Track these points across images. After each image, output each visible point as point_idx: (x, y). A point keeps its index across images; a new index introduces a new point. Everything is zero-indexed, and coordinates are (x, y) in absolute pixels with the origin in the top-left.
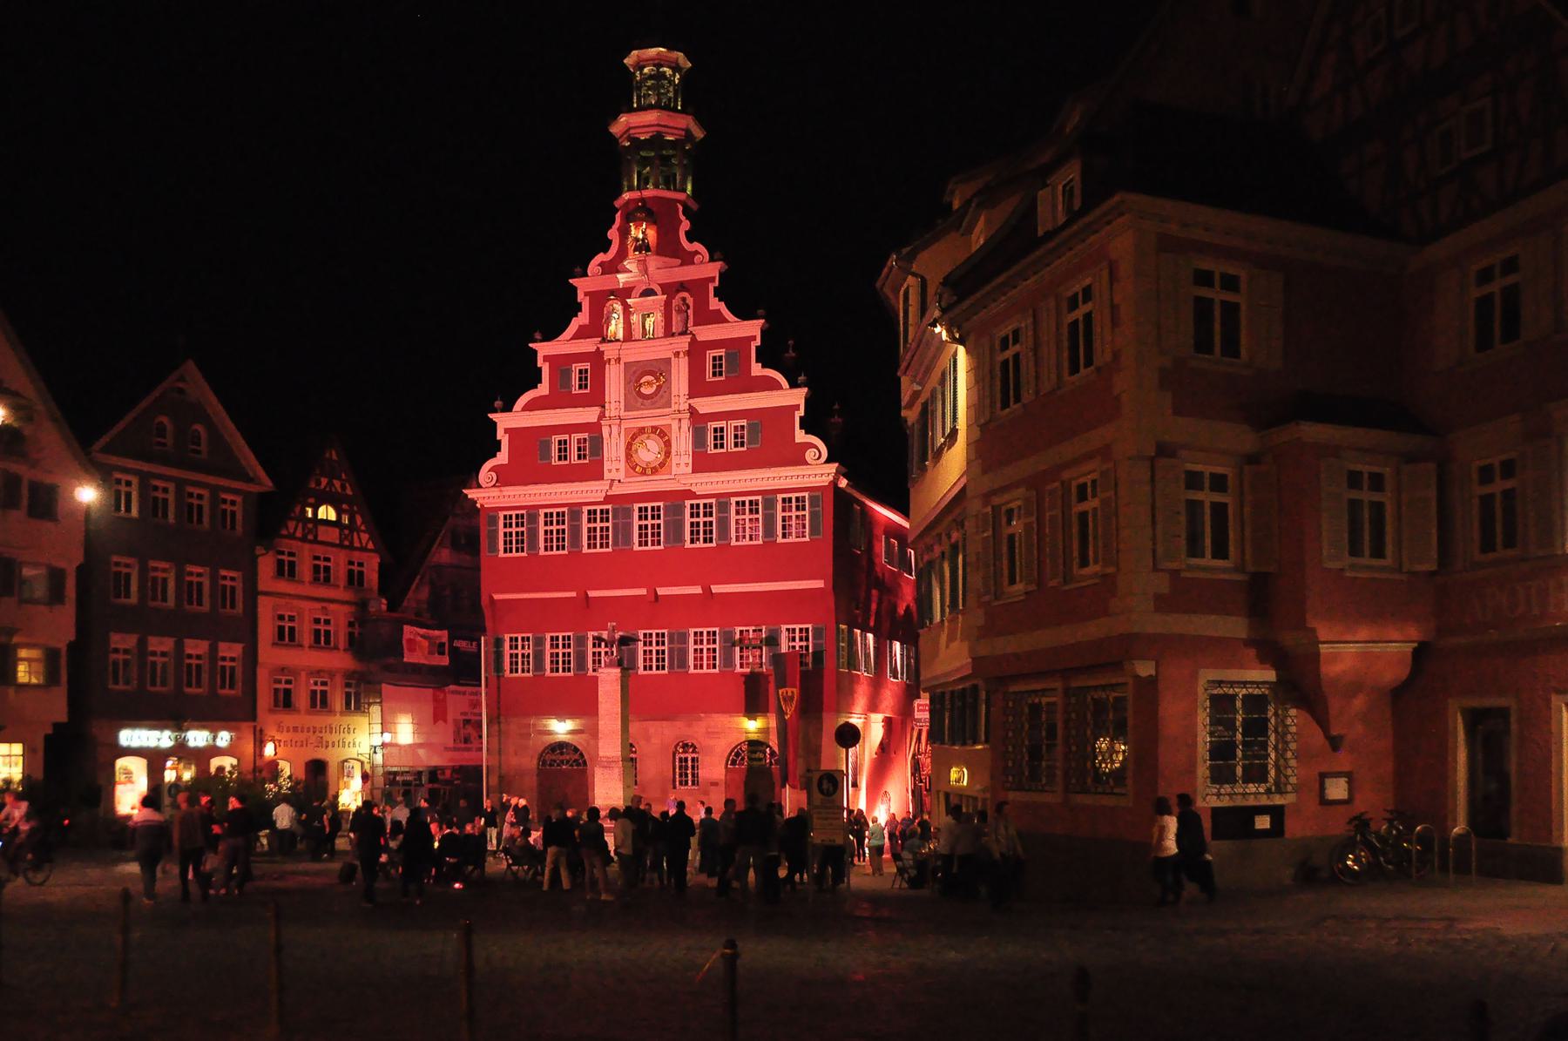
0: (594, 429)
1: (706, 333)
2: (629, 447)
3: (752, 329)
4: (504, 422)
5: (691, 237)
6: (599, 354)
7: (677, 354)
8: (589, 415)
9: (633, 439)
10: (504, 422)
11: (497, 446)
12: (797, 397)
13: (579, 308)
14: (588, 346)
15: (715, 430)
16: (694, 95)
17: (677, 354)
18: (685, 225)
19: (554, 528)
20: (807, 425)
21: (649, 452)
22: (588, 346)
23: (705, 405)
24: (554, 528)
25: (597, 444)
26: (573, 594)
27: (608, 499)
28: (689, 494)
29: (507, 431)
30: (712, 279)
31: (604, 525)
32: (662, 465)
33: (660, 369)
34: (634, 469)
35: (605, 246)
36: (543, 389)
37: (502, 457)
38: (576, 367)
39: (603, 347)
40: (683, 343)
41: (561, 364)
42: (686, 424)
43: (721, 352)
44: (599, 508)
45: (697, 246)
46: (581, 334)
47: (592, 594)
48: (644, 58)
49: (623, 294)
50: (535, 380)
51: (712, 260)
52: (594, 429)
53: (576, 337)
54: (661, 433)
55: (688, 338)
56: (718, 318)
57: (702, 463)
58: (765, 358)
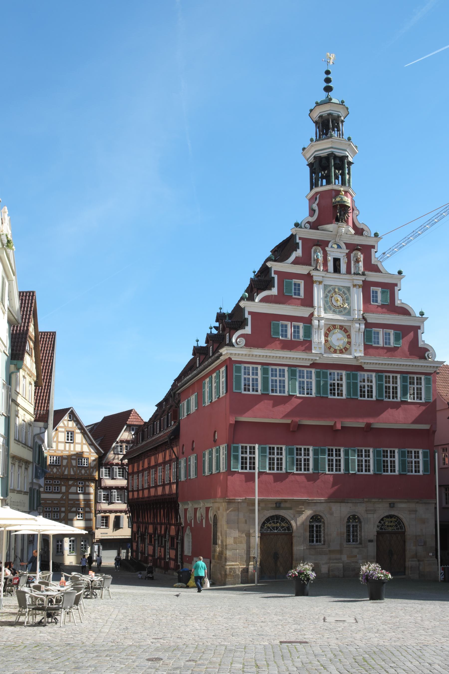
0: (308, 321)
2: (326, 335)
7: (355, 286)
8: (304, 312)
9: (329, 330)
14: (303, 270)
21: (338, 339)
22: (303, 270)
25: (308, 332)
28: (360, 368)
29: (250, 313)
31: (274, 378)
32: (346, 349)
33: (345, 292)
34: (330, 348)
36: (274, 291)
37: (248, 330)
39: (313, 273)
40: (359, 280)
42: (363, 327)
44: (305, 370)
49: (322, 244)
53: (295, 262)
54: (345, 330)
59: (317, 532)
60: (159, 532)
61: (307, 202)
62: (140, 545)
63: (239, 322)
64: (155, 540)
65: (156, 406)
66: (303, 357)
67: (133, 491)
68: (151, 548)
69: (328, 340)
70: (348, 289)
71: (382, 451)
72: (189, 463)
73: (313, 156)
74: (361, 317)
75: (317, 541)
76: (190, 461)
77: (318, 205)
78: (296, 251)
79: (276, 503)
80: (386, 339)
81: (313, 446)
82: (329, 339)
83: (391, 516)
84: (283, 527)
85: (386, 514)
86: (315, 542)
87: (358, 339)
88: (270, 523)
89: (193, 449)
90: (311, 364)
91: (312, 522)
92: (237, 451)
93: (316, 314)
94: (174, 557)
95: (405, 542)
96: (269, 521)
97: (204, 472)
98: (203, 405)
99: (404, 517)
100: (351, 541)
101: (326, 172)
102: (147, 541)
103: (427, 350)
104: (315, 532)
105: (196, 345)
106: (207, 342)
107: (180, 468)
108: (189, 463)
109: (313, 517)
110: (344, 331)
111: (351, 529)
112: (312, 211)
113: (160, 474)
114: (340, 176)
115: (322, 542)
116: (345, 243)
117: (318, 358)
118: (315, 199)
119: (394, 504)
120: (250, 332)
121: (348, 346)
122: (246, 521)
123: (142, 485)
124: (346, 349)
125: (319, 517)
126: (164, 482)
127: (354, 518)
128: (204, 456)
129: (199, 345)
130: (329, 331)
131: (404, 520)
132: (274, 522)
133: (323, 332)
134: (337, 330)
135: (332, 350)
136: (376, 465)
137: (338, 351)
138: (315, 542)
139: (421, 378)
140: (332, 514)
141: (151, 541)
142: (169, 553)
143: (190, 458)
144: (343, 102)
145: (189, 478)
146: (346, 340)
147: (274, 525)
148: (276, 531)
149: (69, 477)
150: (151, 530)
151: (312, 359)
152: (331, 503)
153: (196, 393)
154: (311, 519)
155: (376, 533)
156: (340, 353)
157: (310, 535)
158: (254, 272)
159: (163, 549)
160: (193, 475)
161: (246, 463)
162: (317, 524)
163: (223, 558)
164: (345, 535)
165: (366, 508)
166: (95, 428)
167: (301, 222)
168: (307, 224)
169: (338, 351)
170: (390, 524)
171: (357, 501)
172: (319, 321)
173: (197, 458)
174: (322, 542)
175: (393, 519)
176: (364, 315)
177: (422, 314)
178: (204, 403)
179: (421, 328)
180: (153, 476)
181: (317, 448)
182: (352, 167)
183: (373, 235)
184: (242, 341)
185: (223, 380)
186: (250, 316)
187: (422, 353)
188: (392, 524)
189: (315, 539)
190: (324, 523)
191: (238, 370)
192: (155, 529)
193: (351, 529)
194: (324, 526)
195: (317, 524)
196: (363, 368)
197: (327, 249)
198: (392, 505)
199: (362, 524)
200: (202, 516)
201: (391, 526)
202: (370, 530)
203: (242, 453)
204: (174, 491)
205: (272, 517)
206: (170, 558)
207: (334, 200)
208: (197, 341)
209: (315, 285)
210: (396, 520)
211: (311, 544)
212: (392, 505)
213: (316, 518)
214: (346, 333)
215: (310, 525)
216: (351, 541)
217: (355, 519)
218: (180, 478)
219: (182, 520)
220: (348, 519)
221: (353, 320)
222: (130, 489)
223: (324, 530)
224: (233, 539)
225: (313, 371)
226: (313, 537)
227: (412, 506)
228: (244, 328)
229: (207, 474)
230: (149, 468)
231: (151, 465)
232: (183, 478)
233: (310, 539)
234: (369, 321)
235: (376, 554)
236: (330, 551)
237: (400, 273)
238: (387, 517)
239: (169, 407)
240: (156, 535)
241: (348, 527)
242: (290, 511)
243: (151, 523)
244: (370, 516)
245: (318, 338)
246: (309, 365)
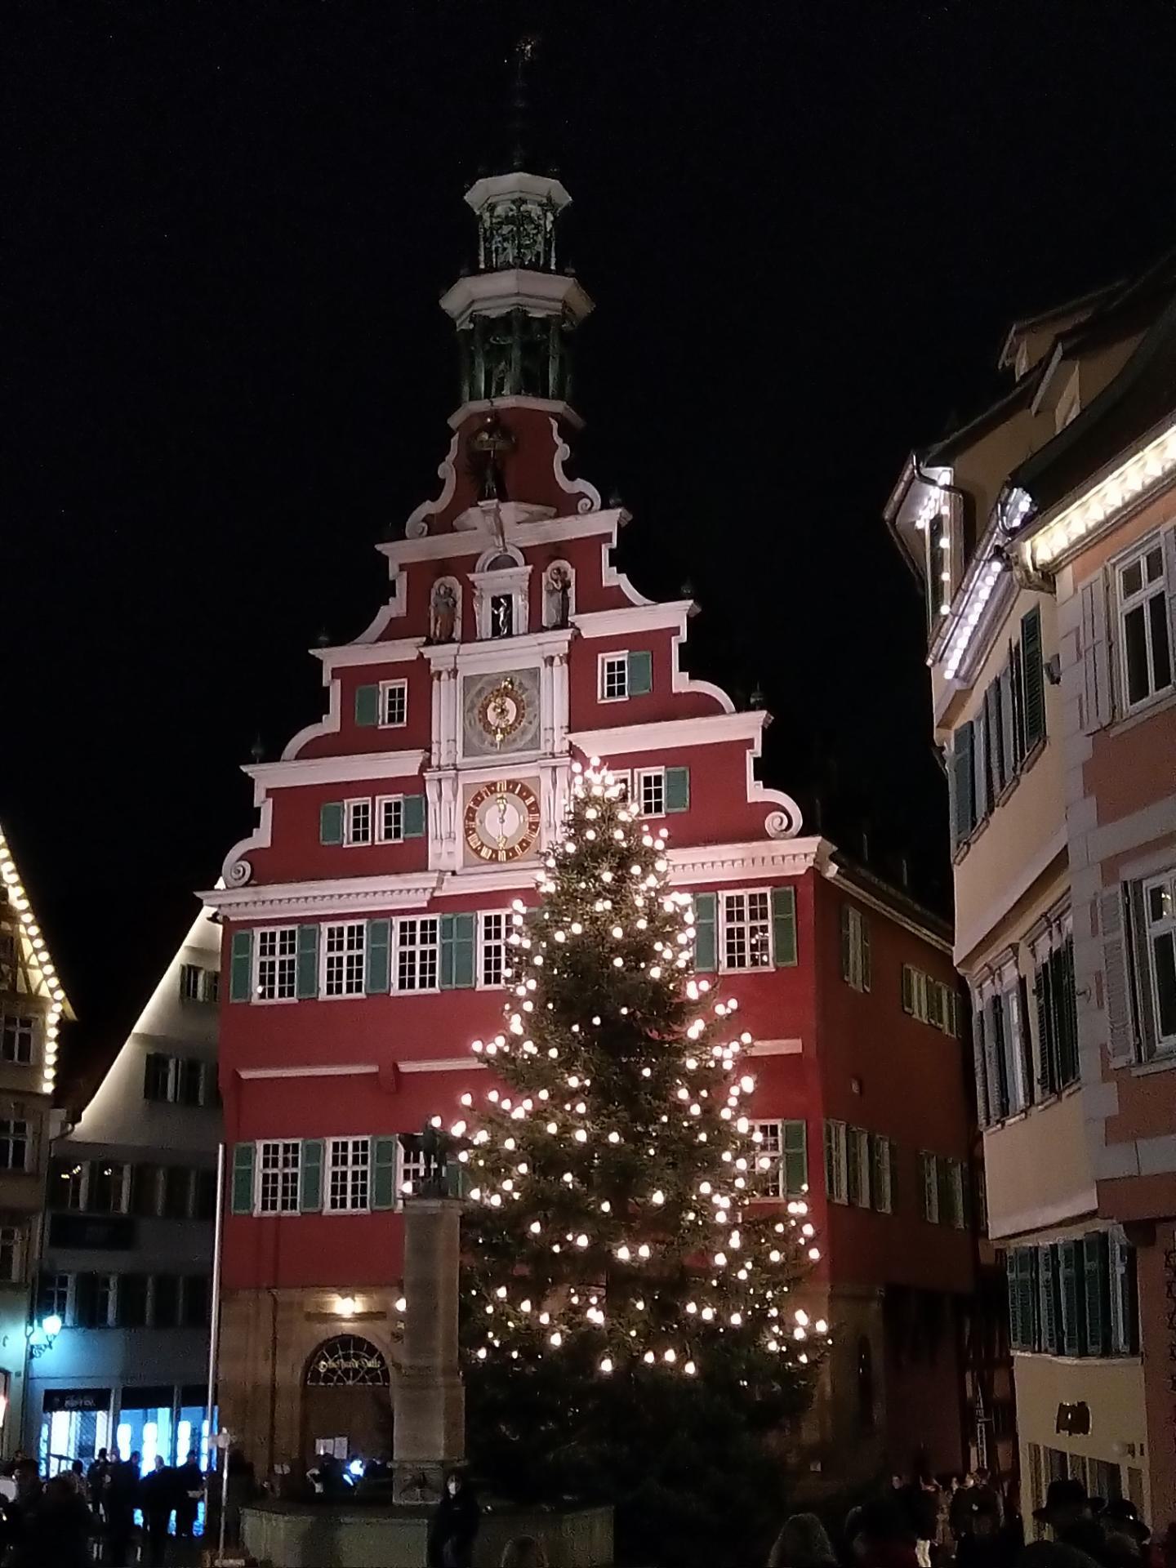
0: (414, 785)
1: (596, 625)
2: (470, 815)
3: (674, 615)
4: (266, 777)
5: (571, 472)
6: (423, 662)
7: (550, 661)
8: (404, 763)
10: (266, 777)
11: (252, 819)
12: (746, 727)
13: (390, 590)
14: (405, 651)
15: (611, 666)
16: (573, 244)
17: (550, 661)
18: (563, 452)
19: (345, 954)
20: (768, 773)
22: (405, 651)
24: (345, 954)
25: (419, 813)
26: (373, 1069)
27: (435, 904)
30: (607, 537)
31: (428, 947)
32: (524, 844)
34: (477, 852)
35: (434, 489)
36: (331, 723)
37: (262, 837)
38: (386, 686)
39: (429, 652)
41: (358, 679)
43: (622, 656)
44: (419, 919)
45: (582, 485)
46: (394, 632)
47: (406, 1067)
48: (495, 192)
50: (319, 709)
51: (605, 506)
52: (414, 785)
54: (523, 791)
55: (567, 634)
56: (616, 600)
58: (694, 664)
66: (246, 899)
69: (474, 830)
70: (534, 673)
93: (434, 762)
110: (519, 794)
116: (521, 549)
120: (267, 843)
130: (477, 802)
147: (344, 1365)
148: (350, 1382)
169: (502, 856)
197: (472, 577)
209: (435, 682)
214: (524, 799)
225: (435, 917)
242: (379, 1323)
246: (425, 905)
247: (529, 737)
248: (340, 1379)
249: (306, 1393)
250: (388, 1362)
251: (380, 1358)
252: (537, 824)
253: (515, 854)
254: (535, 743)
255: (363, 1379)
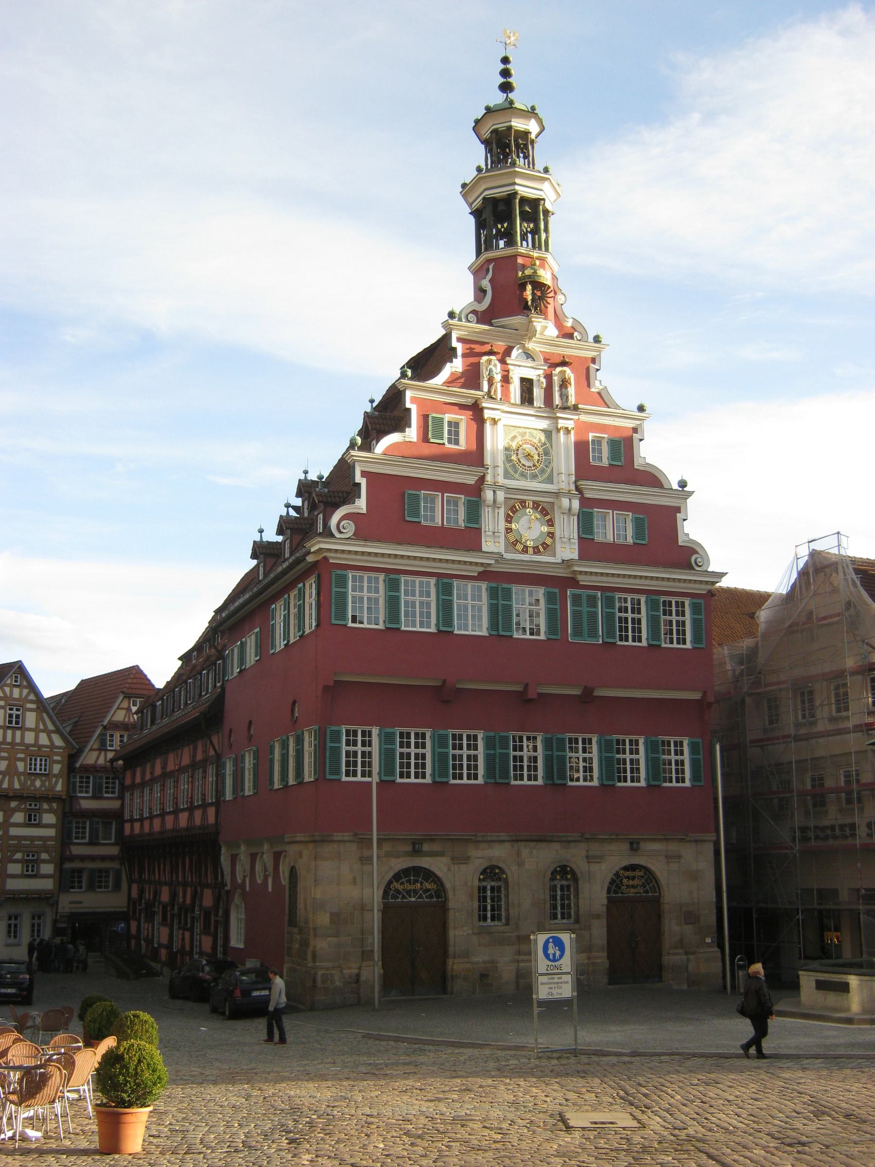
0: (475, 491)
2: (509, 519)
21: (530, 527)
23: (595, 490)
25: (474, 512)
28: (572, 582)
29: (364, 474)
34: (514, 543)
36: (412, 433)
37: (361, 504)
42: (576, 504)
54: (545, 511)
57: (589, 548)
59: (492, 899)
60: (181, 900)
61: (471, 278)
62: (144, 926)
63: (342, 492)
64: (173, 916)
65: (180, 659)
67: (132, 821)
68: (165, 931)
71: (615, 742)
72: (242, 765)
73: (481, 198)
74: (573, 487)
75: (493, 918)
76: (243, 761)
77: (490, 281)
78: (451, 362)
79: (414, 844)
80: (619, 530)
81: (485, 730)
82: (513, 526)
83: (633, 867)
84: (427, 890)
85: (625, 863)
86: (489, 920)
87: (567, 530)
88: (402, 883)
89: (250, 738)
90: (480, 573)
91: (483, 880)
92: (339, 740)
93: (489, 478)
94: (209, 950)
95: (659, 916)
96: (401, 878)
97: (272, 782)
98: (272, 652)
99: (658, 867)
100: (559, 916)
101: (505, 225)
102: (158, 918)
103: (695, 552)
104: (489, 901)
105: (258, 539)
106: (280, 532)
107: (224, 774)
108: (242, 765)
109: (485, 870)
110: (541, 511)
111: (559, 893)
112: (480, 292)
113: (184, 786)
114: (530, 236)
115: (504, 920)
117: (493, 562)
118: (485, 271)
119: (638, 843)
121: (549, 541)
122: (354, 879)
123: (150, 809)
124: (545, 546)
125: (497, 871)
126: (192, 803)
127: (563, 871)
128: (272, 751)
129: (264, 540)
130: (514, 513)
131: (658, 874)
132: (409, 881)
133: (502, 512)
134: (528, 510)
135: (519, 547)
136: (604, 767)
137: (531, 550)
138: (489, 920)
139: (683, 603)
140: (521, 864)
141: (164, 918)
142: (200, 941)
143: (243, 756)
144: (533, 108)
145: (241, 794)
146: (545, 529)
148: (413, 899)
149: (11, 794)
150: (165, 896)
151: (482, 564)
152: (520, 843)
153: (258, 629)
154: (481, 874)
155: (605, 902)
156: (535, 553)
157: (479, 906)
158: (372, 401)
159: (187, 934)
160: (248, 791)
161: (355, 764)
162: (493, 884)
163: (309, 954)
164: (548, 905)
165: (587, 851)
166: (63, 701)
167: (461, 312)
168: (470, 315)
169: (531, 550)
170: (631, 882)
171: (570, 839)
172: (494, 491)
173: (257, 757)
174: (504, 920)
175: (638, 873)
176: (579, 483)
177: (683, 484)
178: (273, 646)
179: (682, 510)
180: (170, 791)
181: (492, 734)
182: (552, 219)
183: (591, 339)
184: (350, 528)
185: (311, 598)
186: (365, 479)
187: (687, 557)
188: (635, 882)
189: (489, 914)
190: (506, 881)
191: (342, 582)
192: (174, 895)
193: (559, 893)
194: (507, 888)
195: (493, 884)
196: (578, 582)
198: (634, 847)
199: (580, 882)
200: (266, 870)
201: (633, 886)
202: (594, 895)
203: (348, 744)
204: (211, 820)
205: (406, 872)
206: (201, 953)
207: (520, 274)
208: (261, 531)
210: (642, 874)
211: (482, 923)
212: (635, 846)
213: (491, 873)
215: (479, 887)
216: (559, 916)
217: (566, 873)
218: (224, 794)
219: (228, 878)
220: (552, 874)
221: (557, 494)
222: (127, 816)
223: (507, 896)
224: (328, 915)
225: (484, 586)
226: (485, 909)
227: (673, 847)
228: (354, 503)
229: (277, 786)
230: (165, 775)
231: (168, 770)
232: (229, 796)
233: (479, 915)
234: (587, 496)
235: (605, 942)
236: (518, 937)
237: (641, 409)
238: (626, 869)
239: (202, 659)
240: (176, 907)
241: (553, 889)
242: (439, 858)
243: (166, 884)
244: (594, 867)
245: (492, 523)
247: (546, 475)
248: (404, 897)
249: (386, 909)
250: (448, 885)
251: (437, 880)
252: (553, 534)
253: (539, 551)
254: (550, 480)
255: (421, 897)
